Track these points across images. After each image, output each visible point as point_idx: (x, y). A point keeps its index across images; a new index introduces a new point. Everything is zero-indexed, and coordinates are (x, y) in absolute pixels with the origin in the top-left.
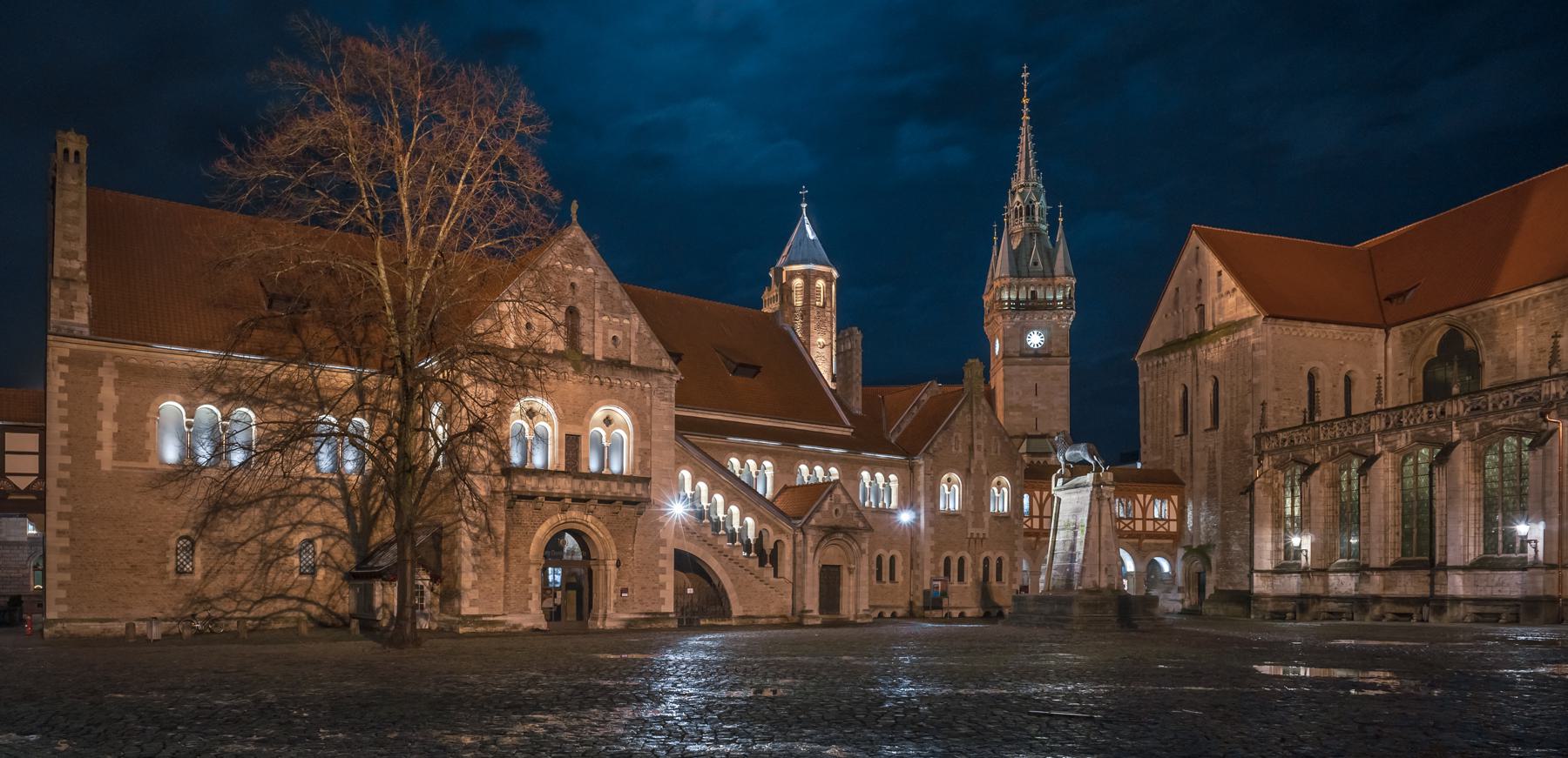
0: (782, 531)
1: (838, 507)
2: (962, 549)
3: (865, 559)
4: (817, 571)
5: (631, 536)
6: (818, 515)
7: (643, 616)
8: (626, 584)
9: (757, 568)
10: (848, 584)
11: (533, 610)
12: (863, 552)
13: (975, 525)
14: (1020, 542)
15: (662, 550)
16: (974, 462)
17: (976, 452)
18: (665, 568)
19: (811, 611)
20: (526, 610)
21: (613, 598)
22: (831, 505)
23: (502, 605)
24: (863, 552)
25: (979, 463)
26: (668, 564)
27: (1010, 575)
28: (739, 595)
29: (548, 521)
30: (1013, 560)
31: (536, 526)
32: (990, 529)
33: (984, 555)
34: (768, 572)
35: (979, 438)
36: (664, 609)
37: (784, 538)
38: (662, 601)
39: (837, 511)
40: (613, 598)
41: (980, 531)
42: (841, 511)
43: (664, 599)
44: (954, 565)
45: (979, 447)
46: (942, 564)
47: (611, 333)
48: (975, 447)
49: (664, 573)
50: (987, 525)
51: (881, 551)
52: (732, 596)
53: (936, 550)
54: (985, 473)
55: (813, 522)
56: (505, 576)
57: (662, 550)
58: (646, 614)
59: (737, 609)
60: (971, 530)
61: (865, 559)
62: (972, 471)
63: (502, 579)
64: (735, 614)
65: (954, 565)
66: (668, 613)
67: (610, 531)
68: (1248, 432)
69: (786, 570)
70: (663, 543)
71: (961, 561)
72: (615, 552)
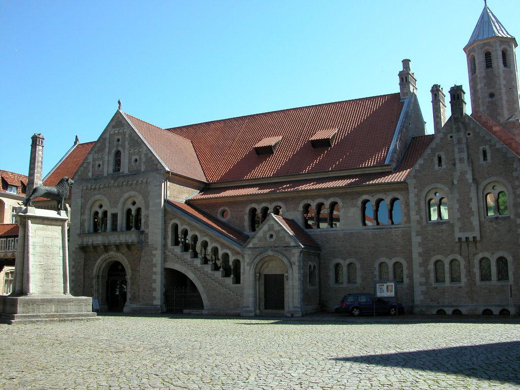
0: (238, 253)
2: (452, 252)
9: (220, 278)
12: (291, 264)
13: (462, 229)
15: (154, 269)
16: (457, 174)
18: (155, 280)
19: (248, 307)
22: (265, 233)
25: (463, 173)
29: (101, 257)
31: (96, 260)
33: (480, 256)
34: (229, 281)
39: (271, 236)
41: (470, 235)
42: (274, 237)
43: (155, 297)
46: (431, 267)
48: (457, 161)
49: (155, 283)
50: (477, 228)
51: (383, 259)
53: (426, 255)
54: (470, 181)
56: (84, 285)
60: (458, 235)
61: (296, 268)
62: (455, 182)
63: (82, 286)
67: (128, 260)
70: (155, 266)
72: (130, 271)
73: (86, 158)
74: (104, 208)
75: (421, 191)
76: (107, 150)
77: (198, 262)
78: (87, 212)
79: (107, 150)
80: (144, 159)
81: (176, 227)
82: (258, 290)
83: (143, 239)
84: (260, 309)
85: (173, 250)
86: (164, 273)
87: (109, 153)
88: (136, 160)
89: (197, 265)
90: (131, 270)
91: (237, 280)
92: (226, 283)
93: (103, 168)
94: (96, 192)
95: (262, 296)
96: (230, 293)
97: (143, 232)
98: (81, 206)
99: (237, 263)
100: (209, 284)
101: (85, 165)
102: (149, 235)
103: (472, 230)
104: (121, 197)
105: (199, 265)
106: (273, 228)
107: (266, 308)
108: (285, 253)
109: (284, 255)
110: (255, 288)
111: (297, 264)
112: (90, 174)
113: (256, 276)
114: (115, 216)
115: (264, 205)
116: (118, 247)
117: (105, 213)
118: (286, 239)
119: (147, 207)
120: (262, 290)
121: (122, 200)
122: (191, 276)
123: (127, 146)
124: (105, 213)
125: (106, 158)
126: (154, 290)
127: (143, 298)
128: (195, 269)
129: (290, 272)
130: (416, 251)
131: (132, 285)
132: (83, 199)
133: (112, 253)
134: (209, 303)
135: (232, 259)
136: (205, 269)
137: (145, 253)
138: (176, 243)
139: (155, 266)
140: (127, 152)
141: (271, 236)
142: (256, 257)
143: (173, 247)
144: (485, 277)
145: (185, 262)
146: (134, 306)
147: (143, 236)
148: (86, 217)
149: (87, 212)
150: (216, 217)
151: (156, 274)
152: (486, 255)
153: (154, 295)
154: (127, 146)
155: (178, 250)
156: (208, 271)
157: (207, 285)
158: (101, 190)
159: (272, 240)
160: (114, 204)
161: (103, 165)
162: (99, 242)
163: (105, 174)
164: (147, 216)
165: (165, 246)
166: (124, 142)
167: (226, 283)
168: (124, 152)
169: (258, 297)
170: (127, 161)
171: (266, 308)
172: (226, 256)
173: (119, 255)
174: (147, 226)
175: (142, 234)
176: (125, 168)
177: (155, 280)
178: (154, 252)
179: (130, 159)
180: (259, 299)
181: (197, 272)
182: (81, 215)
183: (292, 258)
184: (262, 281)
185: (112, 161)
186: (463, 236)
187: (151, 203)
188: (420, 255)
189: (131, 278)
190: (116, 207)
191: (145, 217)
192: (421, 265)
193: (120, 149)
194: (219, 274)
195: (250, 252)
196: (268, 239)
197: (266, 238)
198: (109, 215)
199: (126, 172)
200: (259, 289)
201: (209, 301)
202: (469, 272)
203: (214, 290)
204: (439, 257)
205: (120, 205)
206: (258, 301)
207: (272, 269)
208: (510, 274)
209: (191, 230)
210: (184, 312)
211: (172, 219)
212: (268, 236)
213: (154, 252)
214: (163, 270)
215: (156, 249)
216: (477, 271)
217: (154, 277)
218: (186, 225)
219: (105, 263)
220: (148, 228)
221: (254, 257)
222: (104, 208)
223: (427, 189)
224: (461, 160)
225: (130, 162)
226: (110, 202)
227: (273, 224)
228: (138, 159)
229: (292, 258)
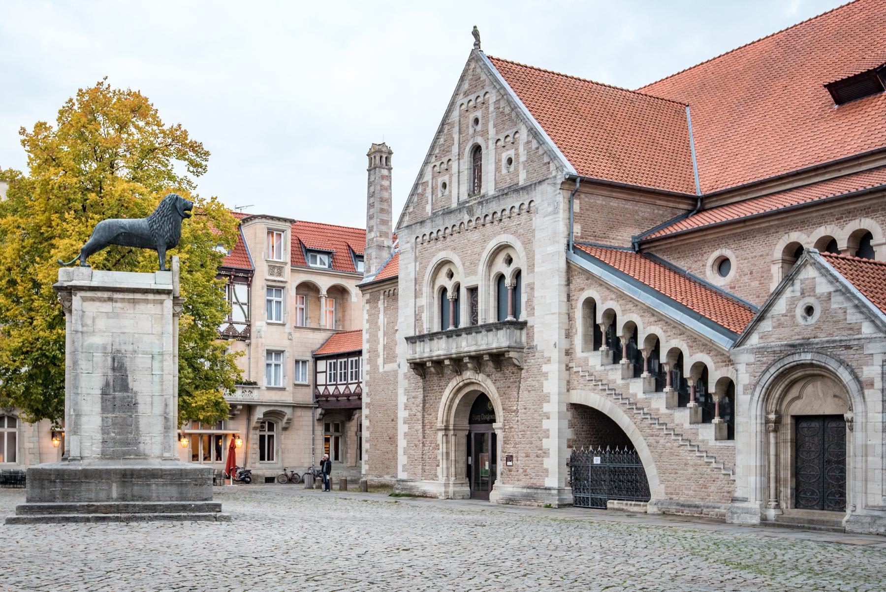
1: (810, 301)
5: (515, 394)
6: (766, 326)
7: (525, 491)
8: (511, 450)
11: (440, 477)
12: (862, 385)
15: (547, 408)
18: (548, 430)
22: (793, 303)
23: (420, 471)
24: (862, 385)
28: (659, 468)
39: (809, 310)
42: (817, 313)
49: (548, 437)
57: (547, 408)
58: (528, 488)
64: (653, 498)
66: (549, 489)
70: (546, 398)
73: (421, 174)
74: (456, 279)
76: (455, 149)
78: (426, 289)
79: (455, 149)
80: (523, 158)
81: (591, 305)
82: (772, 459)
83: (524, 339)
84: (778, 506)
85: (586, 360)
86: (569, 415)
87: (460, 156)
89: (635, 395)
90: (504, 409)
92: (700, 438)
93: (450, 192)
94: (440, 244)
95: (787, 474)
96: (709, 463)
97: (522, 325)
98: (415, 279)
99: (728, 387)
100: (662, 441)
101: (420, 191)
102: (535, 330)
104: (483, 248)
106: (813, 289)
107: (797, 505)
108: (844, 354)
109: (841, 362)
110: (765, 452)
111: (878, 384)
112: (429, 208)
113: (767, 421)
114: (473, 291)
116: (477, 360)
117: (457, 288)
118: (848, 317)
119: (531, 267)
120: (787, 455)
123: (492, 131)
124: (457, 288)
125: (454, 166)
126: (546, 453)
127: (525, 471)
129: (858, 407)
131: (505, 442)
132: (418, 264)
133: (468, 375)
134: (663, 486)
135: (715, 375)
136: (654, 405)
137: (527, 372)
139: (546, 398)
140: (491, 145)
141: (809, 310)
142: (767, 369)
143: (585, 355)
145: (611, 391)
147: (524, 332)
148: (423, 301)
150: (701, 277)
151: (548, 418)
153: (545, 466)
154: (492, 131)
155: (596, 360)
156: (658, 409)
157: (657, 442)
158: (448, 240)
159: (812, 320)
161: (450, 182)
162: (441, 352)
163: (454, 205)
164: (531, 287)
165: (568, 353)
166: (486, 124)
167: (700, 438)
168: (487, 148)
169: (772, 475)
171: (797, 505)
173: (480, 377)
174: (531, 310)
175: (521, 329)
177: (548, 430)
178: (545, 368)
179: (498, 162)
180: (777, 480)
181: (635, 411)
182: (416, 297)
183: (865, 369)
184: (787, 433)
185: (466, 172)
187: (538, 257)
190: (474, 273)
191: (528, 289)
193: (480, 140)
195: (751, 358)
196: (800, 320)
197: (794, 317)
200: (777, 456)
201: (662, 482)
203: (672, 454)
205: (481, 268)
206: (772, 485)
209: (624, 311)
210: (609, 505)
211: (582, 289)
212: (800, 311)
214: (565, 409)
215: (549, 360)
217: (546, 424)
218: (612, 299)
219: (460, 396)
220: (533, 315)
221: (764, 368)
225: (498, 169)
226: (463, 264)
227: (814, 278)
228: (513, 159)
229: (865, 369)
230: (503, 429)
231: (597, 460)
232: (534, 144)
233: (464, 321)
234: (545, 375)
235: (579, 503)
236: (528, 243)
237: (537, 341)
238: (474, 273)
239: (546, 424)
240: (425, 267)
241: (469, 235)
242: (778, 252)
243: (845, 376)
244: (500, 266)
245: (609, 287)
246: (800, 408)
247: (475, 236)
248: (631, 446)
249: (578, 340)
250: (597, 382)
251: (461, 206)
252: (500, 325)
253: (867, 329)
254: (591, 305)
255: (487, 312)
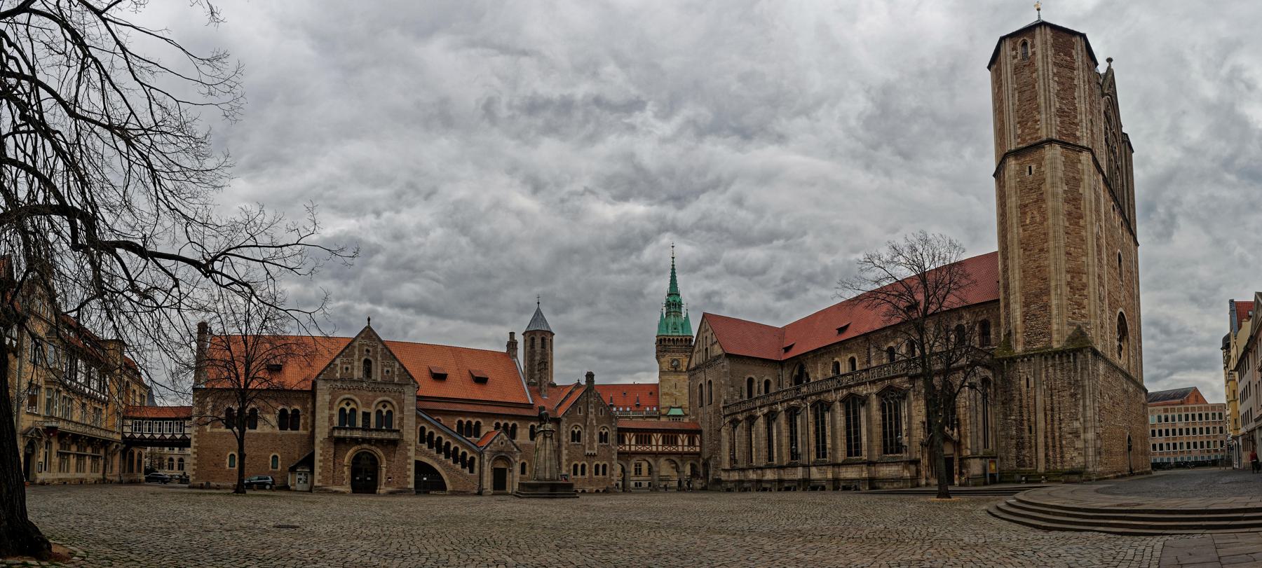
3: (517, 464)
4: (490, 470)
6: (492, 445)
8: (390, 475)
10: (509, 477)
13: (589, 449)
14: (615, 457)
15: (408, 461)
16: (589, 420)
17: (590, 415)
20: (342, 484)
21: (384, 481)
22: (498, 441)
25: (592, 420)
26: (412, 467)
27: (610, 472)
30: (612, 465)
32: (598, 451)
33: (596, 463)
35: (592, 407)
36: (409, 486)
37: (475, 456)
38: (409, 483)
39: (502, 443)
40: (384, 481)
44: (579, 468)
45: (591, 413)
46: (572, 467)
47: (385, 369)
52: (447, 482)
53: (569, 461)
55: (488, 448)
57: (408, 461)
59: (449, 487)
60: (587, 451)
64: (448, 489)
65: (579, 468)
68: (721, 406)
69: (476, 470)
70: (409, 458)
71: (583, 466)
75: (569, 425)
77: (442, 457)
80: (397, 373)
81: (423, 429)
88: (388, 371)
91: (472, 471)
99: (472, 459)
103: (594, 449)
105: (444, 459)
114: (366, 416)
115: (469, 419)
119: (402, 411)
121: (375, 402)
122: (437, 467)
124: (353, 410)
126: (409, 476)
128: (440, 462)
130: (564, 458)
133: (365, 446)
138: (422, 441)
144: (597, 473)
145: (431, 457)
146: (390, 489)
149: (335, 408)
152: (599, 462)
158: (352, 391)
160: (368, 405)
164: (402, 419)
170: (379, 371)
172: (464, 454)
173: (373, 448)
176: (377, 375)
178: (408, 447)
186: (589, 452)
187: (406, 409)
188: (567, 460)
189: (386, 467)
190: (370, 408)
192: (567, 466)
194: (459, 466)
198: (360, 413)
199: (379, 380)
202: (590, 471)
204: (576, 462)
205: (373, 406)
207: (501, 465)
208: (608, 472)
213: (408, 447)
215: (410, 445)
216: (594, 470)
222: (353, 406)
223: (573, 425)
224: (591, 413)
230: (386, 467)
231: (425, 479)
232: (402, 370)
233: (360, 423)
234: (409, 450)
235: (418, 493)
236: (401, 403)
237: (405, 438)
238: (370, 408)
239: (408, 467)
240: (336, 399)
241: (365, 392)
242: (456, 421)
243: (512, 459)
244: (380, 407)
245: (432, 424)
246: (496, 466)
247: (370, 394)
248: (439, 473)
249: (418, 440)
250: (426, 454)
251: (361, 381)
252: (378, 430)
253: (515, 450)
254: (423, 429)
255: (373, 425)
